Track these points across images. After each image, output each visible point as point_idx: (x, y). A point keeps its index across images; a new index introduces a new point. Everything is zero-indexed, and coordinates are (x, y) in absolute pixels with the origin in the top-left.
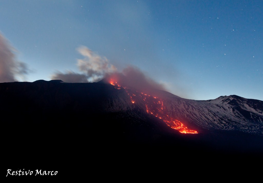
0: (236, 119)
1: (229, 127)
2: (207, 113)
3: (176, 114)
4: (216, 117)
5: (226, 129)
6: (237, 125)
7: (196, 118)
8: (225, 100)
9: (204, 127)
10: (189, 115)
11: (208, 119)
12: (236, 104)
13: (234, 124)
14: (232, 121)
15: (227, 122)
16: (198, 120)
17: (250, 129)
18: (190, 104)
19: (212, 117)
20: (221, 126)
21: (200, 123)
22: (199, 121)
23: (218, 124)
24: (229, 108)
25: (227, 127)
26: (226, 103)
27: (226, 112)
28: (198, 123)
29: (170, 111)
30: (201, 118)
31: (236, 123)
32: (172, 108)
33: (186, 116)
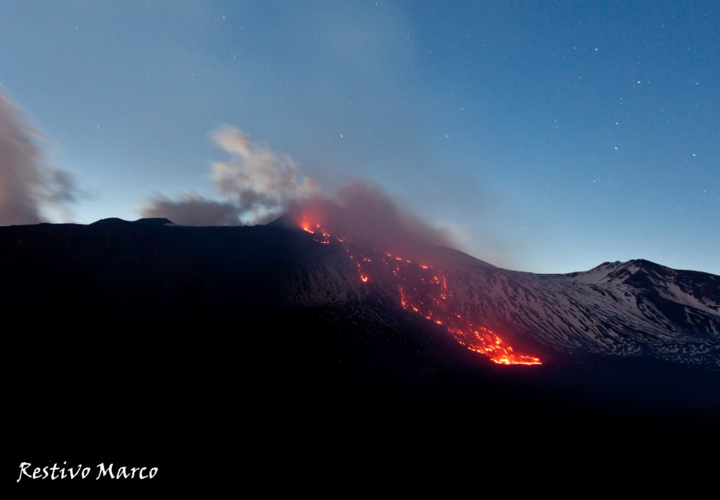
0: (647, 324)
1: (626, 347)
2: (567, 309)
3: (481, 312)
4: (592, 318)
5: (620, 353)
6: (649, 340)
7: (536, 323)
8: (617, 274)
9: (560, 346)
10: (516, 314)
11: (570, 325)
12: (647, 284)
13: (641, 339)
14: (634, 331)
15: (620, 334)
16: (542, 328)
17: (684, 352)
18: (519, 285)
19: (580, 321)
20: (605, 345)
21: (548, 335)
22: (545, 330)
23: (596, 338)
24: (626, 294)
25: (622, 347)
26: (618, 281)
27: (618, 305)
28: (543, 336)
29: (466, 303)
30: (549, 322)
31: (645, 335)
32: (472, 296)
33: (509, 317)
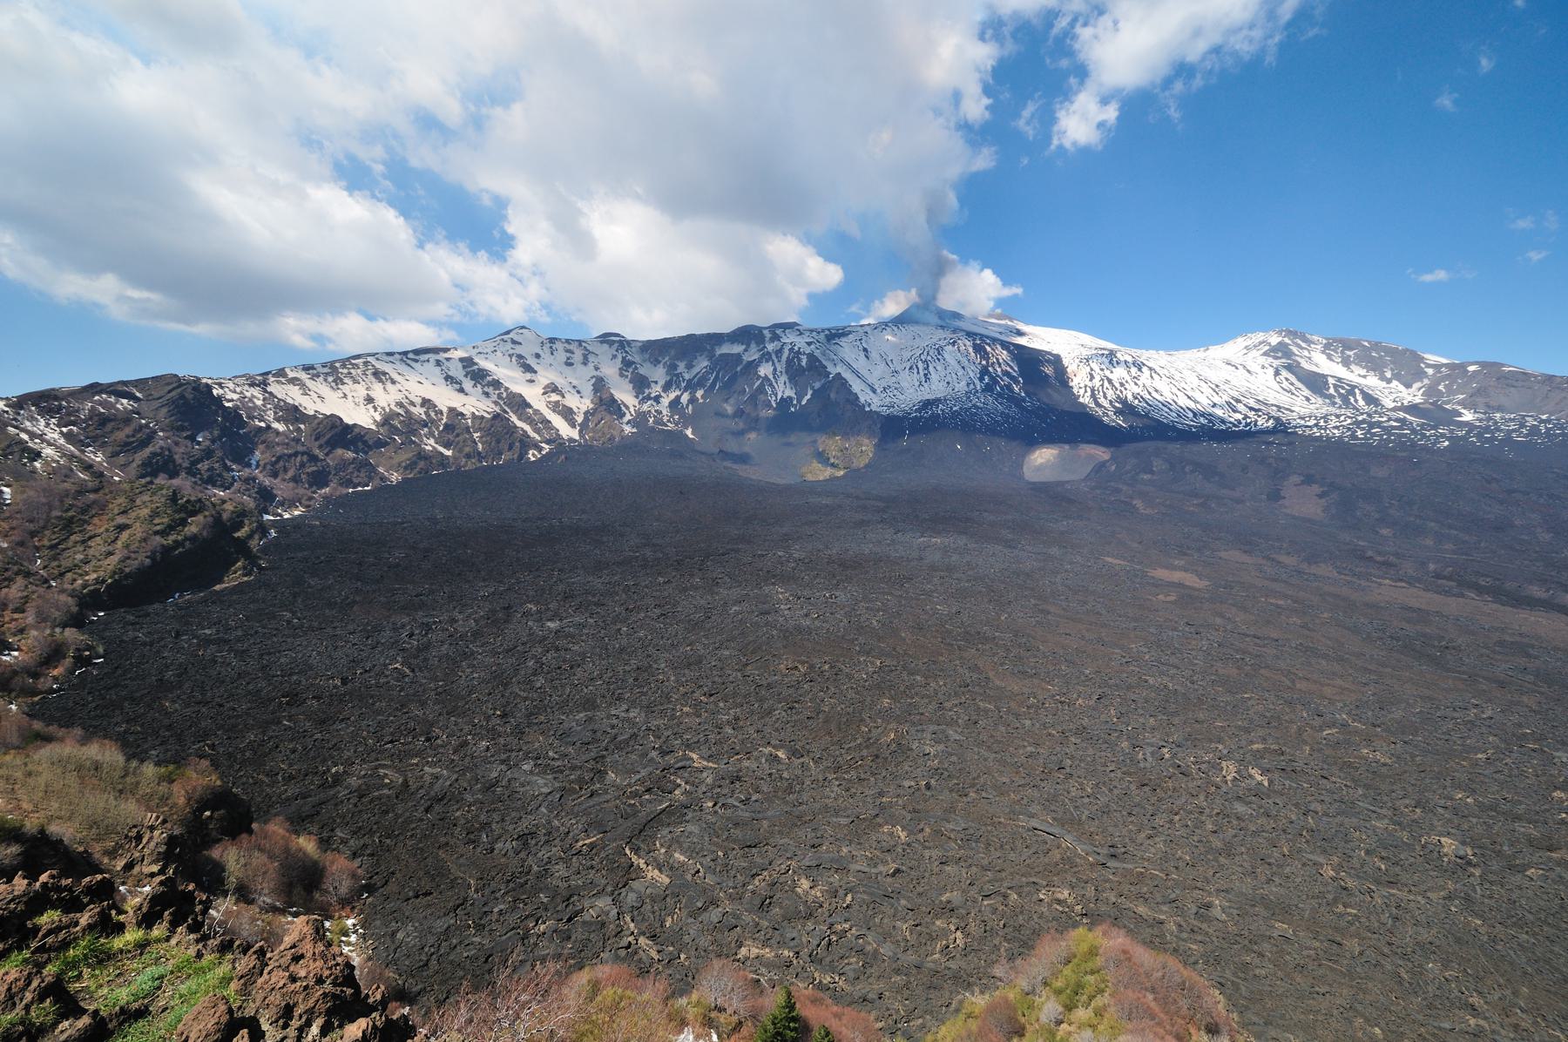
11: (1196, 402)
12: (1288, 354)
27: (1252, 378)
32: (1092, 378)
33: (1130, 397)
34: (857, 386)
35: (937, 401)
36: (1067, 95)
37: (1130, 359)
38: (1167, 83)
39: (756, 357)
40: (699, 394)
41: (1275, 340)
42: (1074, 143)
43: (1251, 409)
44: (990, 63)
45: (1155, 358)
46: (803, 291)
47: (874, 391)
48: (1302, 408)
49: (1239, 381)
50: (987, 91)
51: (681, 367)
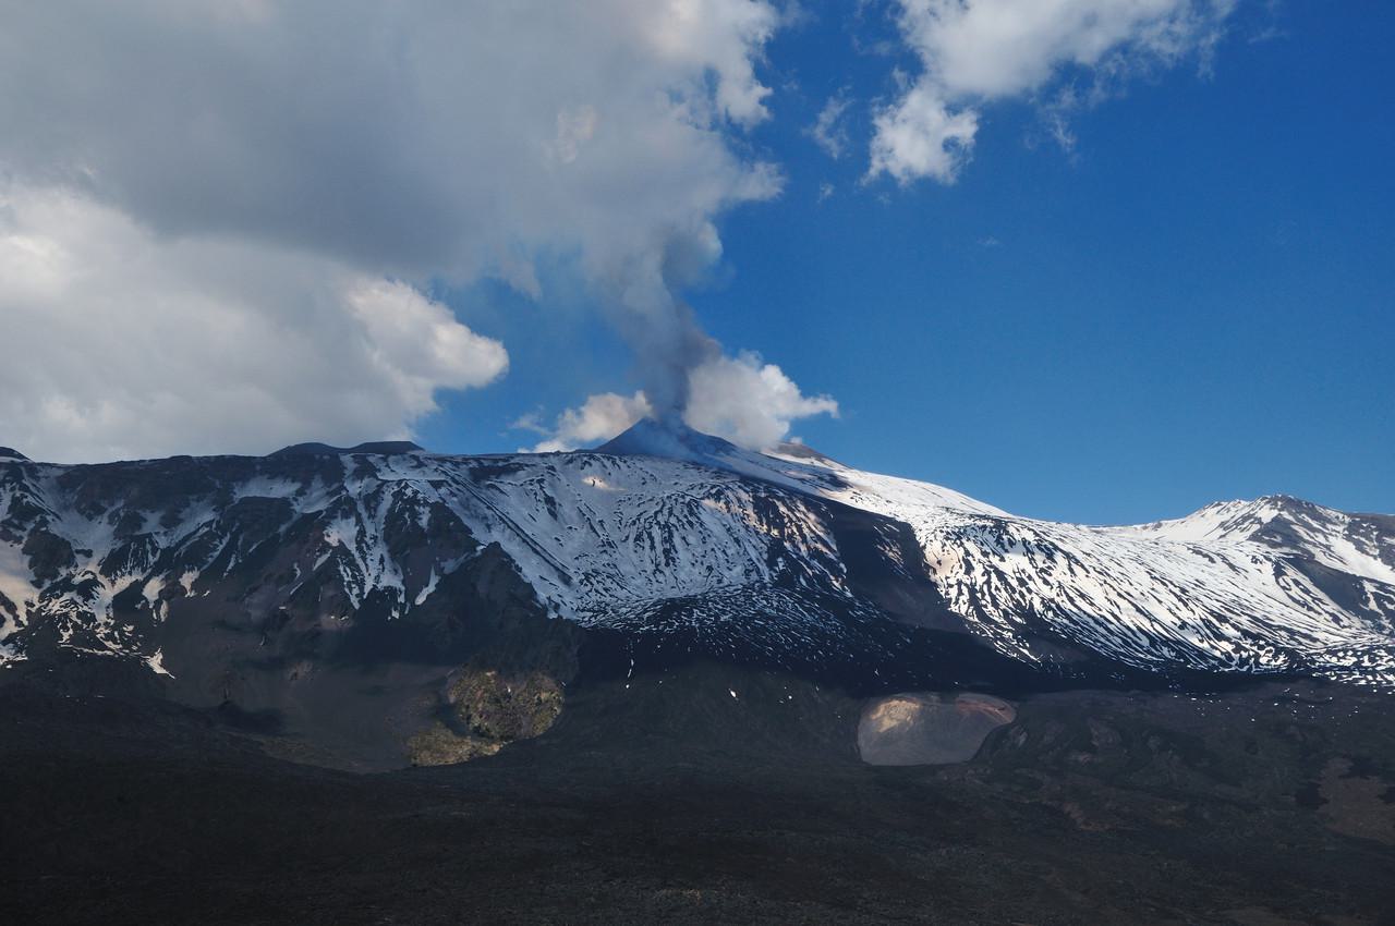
0: (1296, 615)
1: (1257, 656)
3: (988, 597)
4: (1191, 605)
5: (1245, 669)
6: (1300, 644)
7: (1089, 616)
9: (1134, 658)
10: (1052, 600)
11: (1152, 619)
12: (1292, 540)
13: (1283, 639)
16: (1101, 624)
18: (1056, 548)
19: (1170, 610)
20: (1217, 654)
21: (1111, 638)
24: (1255, 560)
25: (1249, 657)
27: (1239, 580)
28: (1102, 640)
29: (959, 583)
30: (1113, 614)
31: (1292, 633)
32: (969, 569)
33: (1038, 606)
34: (531, 570)
35: (688, 603)
36: (892, 96)
37: (1030, 537)
38: (1050, 92)
39: (322, 506)
40: (187, 580)
41: (1267, 514)
42: (908, 171)
43: (1246, 634)
44: (762, 34)
45: (1077, 538)
46: (426, 384)
47: (566, 580)
48: (1330, 634)
49: (1218, 580)
50: (761, 75)
51: (152, 522)
